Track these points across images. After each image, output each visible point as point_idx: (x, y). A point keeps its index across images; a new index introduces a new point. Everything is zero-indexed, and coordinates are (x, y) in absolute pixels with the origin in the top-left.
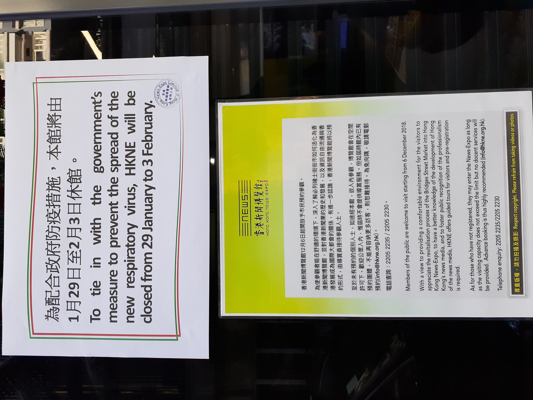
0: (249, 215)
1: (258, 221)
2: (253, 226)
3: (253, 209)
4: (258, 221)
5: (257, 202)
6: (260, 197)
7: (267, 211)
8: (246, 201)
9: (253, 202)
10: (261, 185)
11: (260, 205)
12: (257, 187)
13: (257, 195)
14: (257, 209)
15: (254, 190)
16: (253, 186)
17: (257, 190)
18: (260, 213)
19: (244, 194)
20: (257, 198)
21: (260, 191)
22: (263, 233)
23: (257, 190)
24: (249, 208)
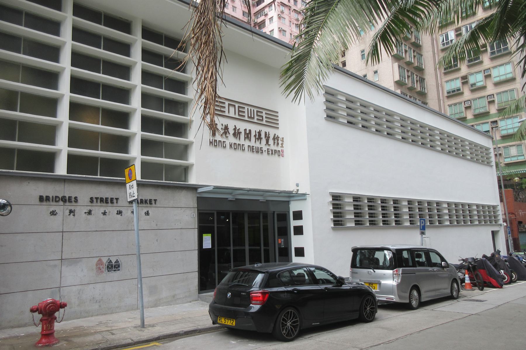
0: (237, 116)
1: (231, 131)
5: (257, 134)
6: (264, 141)
8: (256, 117)
10: (278, 144)
11: (253, 139)
12: (276, 138)
13: (266, 136)
14: (248, 132)
15: (272, 132)
17: (272, 137)
18: (242, 136)
20: (263, 136)
21: (271, 142)
22: (214, 134)
23: (272, 137)
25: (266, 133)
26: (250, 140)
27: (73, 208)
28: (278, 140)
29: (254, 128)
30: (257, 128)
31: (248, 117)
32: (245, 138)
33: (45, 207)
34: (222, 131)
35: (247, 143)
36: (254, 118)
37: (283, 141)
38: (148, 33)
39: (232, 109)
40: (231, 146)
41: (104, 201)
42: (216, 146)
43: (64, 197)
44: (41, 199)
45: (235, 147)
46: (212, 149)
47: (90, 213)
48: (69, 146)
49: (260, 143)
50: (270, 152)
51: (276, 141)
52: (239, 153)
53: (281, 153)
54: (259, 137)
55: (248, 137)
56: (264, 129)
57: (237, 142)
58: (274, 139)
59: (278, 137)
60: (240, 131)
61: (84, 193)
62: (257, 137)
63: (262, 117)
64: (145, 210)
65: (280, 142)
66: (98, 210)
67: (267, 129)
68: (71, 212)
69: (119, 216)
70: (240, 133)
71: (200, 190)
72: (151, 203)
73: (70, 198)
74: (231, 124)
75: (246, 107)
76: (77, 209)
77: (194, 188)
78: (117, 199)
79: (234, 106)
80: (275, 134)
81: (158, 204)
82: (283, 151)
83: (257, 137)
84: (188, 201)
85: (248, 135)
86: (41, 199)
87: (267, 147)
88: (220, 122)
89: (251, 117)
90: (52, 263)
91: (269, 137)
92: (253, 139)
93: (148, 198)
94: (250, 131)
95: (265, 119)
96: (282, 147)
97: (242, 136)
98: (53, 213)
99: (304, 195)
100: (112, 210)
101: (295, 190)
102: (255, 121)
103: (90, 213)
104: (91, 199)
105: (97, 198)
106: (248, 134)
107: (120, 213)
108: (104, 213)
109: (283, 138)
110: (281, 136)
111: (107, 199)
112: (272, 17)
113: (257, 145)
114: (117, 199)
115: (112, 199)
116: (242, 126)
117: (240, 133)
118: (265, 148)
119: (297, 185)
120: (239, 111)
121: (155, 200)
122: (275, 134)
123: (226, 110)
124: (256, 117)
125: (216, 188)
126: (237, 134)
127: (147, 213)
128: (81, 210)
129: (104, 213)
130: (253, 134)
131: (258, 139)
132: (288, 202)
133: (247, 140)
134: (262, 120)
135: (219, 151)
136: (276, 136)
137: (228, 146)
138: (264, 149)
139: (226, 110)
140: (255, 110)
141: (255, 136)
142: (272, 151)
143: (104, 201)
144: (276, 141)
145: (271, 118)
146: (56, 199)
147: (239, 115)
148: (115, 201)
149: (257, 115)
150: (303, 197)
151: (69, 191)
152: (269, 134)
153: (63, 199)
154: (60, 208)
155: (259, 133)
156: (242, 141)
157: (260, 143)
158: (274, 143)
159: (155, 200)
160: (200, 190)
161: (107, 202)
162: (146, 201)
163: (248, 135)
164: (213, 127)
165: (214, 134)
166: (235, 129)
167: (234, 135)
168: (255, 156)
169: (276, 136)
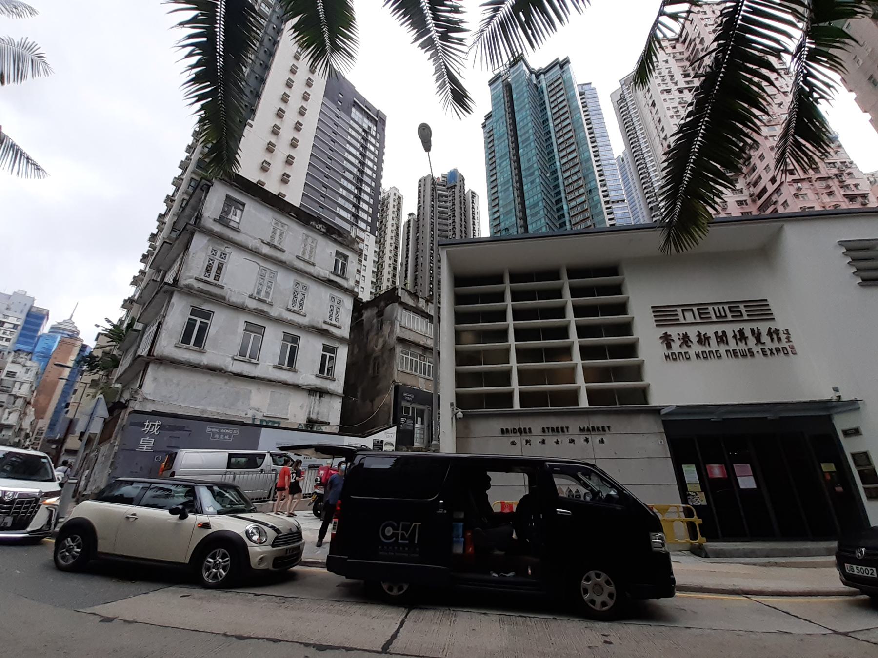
0: (699, 320)
1: (694, 338)
2: (682, 330)
3: (720, 328)
4: (694, 338)
6: (752, 341)
7: (724, 354)
8: (729, 315)
9: (737, 327)
10: (779, 340)
14: (720, 334)
15: (764, 327)
16: (773, 325)
19: (743, 310)
20: (748, 333)
21: (765, 338)
22: (669, 347)
24: (714, 319)
25: (752, 330)
26: (727, 343)
27: (528, 438)
28: (778, 334)
29: (730, 329)
30: (737, 327)
31: (717, 317)
32: (718, 343)
33: (506, 439)
34: (680, 343)
35: (722, 349)
36: (726, 316)
37: (788, 333)
38: (573, 273)
39: (687, 314)
40: (698, 355)
41: (555, 430)
42: (675, 359)
43: (514, 429)
44: (502, 431)
45: (705, 356)
46: (671, 364)
47: (543, 442)
48: (520, 385)
49: (746, 344)
50: (769, 352)
51: (775, 336)
52: (713, 362)
53: (789, 350)
54: (741, 337)
55: (722, 341)
56: (747, 328)
57: (707, 349)
58: (770, 333)
59: (777, 332)
60: (708, 335)
61: (536, 425)
62: (738, 337)
63: (740, 311)
64: (599, 438)
65: (783, 337)
66: (551, 439)
67: (754, 325)
68: (527, 441)
69: (572, 444)
70: (708, 339)
71: (663, 412)
72: (604, 430)
73: (525, 429)
74: (692, 332)
75: (710, 308)
76: (532, 439)
77: (656, 411)
78: (567, 428)
79: (692, 310)
80: (770, 328)
81: (613, 431)
82: (792, 348)
83: (738, 337)
84: (654, 426)
85: (722, 338)
86: (502, 431)
87: (761, 346)
88: (674, 332)
89: (721, 316)
90: (517, 488)
91: (759, 334)
92: (732, 342)
93: (600, 425)
94: (724, 332)
95: (745, 314)
96: (789, 341)
97: (713, 341)
98: (513, 443)
99: (854, 402)
100: (564, 439)
101: (835, 398)
102: (730, 318)
103: (543, 442)
104: (543, 429)
105: (548, 428)
106: (721, 337)
107: (572, 441)
108: (557, 442)
109: (787, 330)
110: (781, 329)
111: (557, 428)
112: (786, 201)
113: (742, 346)
114: (567, 428)
115: (562, 428)
116: (709, 330)
117: (708, 339)
118: (756, 349)
119: (836, 390)
120: (700, 314)
121: (609, 427)
122: (770, 328)
123: (681, 317)
124: (729, 315)
125: (678, 406)
126: (703, 340)
127: (602, 441)
128: (536, 441)
129: (557, 442)
130: (730, 335)
131: (741, 340)
132: (829, 418)
133: (722, 345)
134: (742, 315)
135: (681, 364)
136: (773, 330)
137: (693, 357)
138: (754, 351)
139: (681, 317)
140: (726, 307)
141: (735, 336)
142: (771, 350)
143: (555, 430)
144: (775, 336)
145: (760, 310)
146: (514, 431)
147: (701, 318)
148: (565, 430)
149: (731, 312)
150: (853, 406)
151: (523, 423)
152: (758, 330)
153: (520, 430)
154: (517, 439)
155: (741, 332)
156: (714, 345)
157: (746, 344)
158: (772, 340)
159: (609, 427)
160: (663, 412)
161: (558, 431)
162: (598, 429)
163: (722, 338)
164: (667, 340)
165: (669, 347)
166: (699, 335)
167: (700, 342)
168: (741, 360)
169: (773, 330)
